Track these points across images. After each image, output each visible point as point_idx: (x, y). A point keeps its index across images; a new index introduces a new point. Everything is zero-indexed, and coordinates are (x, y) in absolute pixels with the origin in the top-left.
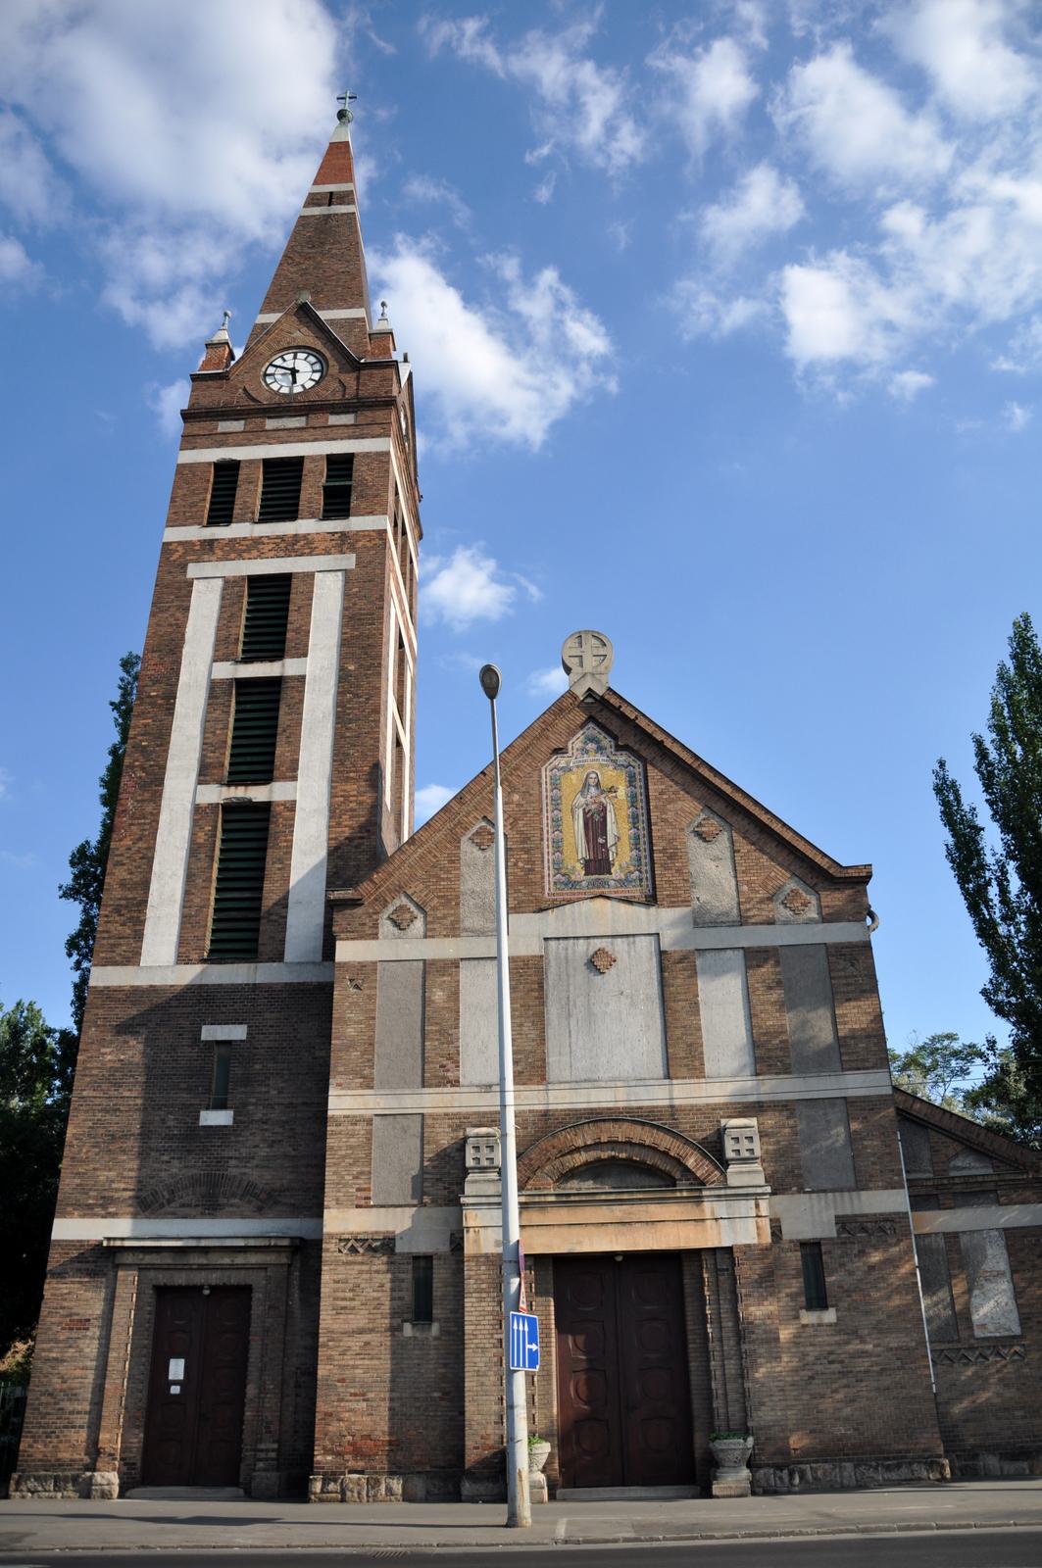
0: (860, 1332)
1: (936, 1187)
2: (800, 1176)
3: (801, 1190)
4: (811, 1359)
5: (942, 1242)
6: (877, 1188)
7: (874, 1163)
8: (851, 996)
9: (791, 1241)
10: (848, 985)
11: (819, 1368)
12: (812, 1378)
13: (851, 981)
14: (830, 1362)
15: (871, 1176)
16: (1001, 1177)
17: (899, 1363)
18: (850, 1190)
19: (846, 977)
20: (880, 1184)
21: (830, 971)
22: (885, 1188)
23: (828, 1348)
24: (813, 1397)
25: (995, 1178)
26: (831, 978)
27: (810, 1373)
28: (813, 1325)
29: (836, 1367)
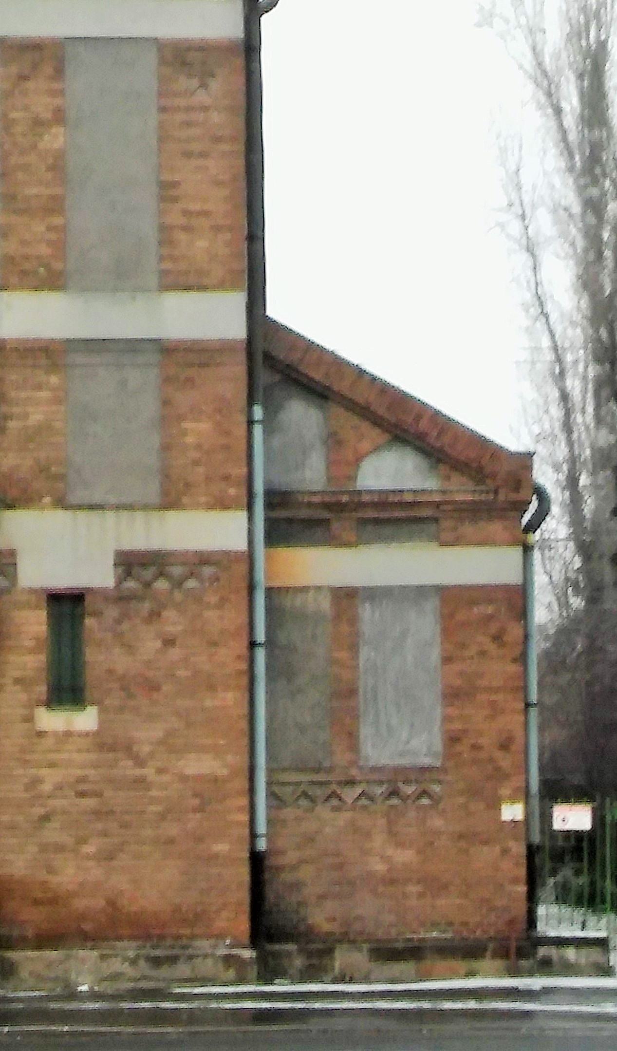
0: (135, 748)
1: (327, 506)
2: (62, 477)
3: (61, 503)
4: (47, 787)
5: (325, 604)
6: (196, 506)
7: (196, 463)
8: (196, 147)
9: (32, 591)
10: (188, 124)
11: (58, 803)
12: (46, 818)
13: (200, 117)
14: (82, 794)
15: (187, 485)
16: (447, 498)
17: (196, 802)
18: (146, 507)
19: (189, 109)
20: (203, 499)
21: (161, 94)
22: (210, 507)
23: (80, 772)
24: (44, 848)
25: (437, 498)
26: (163, 110)
27: (41, 811)
28: (55, 734)
29: (90, 803)
